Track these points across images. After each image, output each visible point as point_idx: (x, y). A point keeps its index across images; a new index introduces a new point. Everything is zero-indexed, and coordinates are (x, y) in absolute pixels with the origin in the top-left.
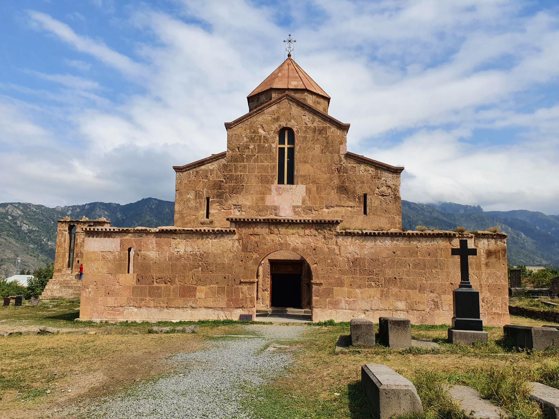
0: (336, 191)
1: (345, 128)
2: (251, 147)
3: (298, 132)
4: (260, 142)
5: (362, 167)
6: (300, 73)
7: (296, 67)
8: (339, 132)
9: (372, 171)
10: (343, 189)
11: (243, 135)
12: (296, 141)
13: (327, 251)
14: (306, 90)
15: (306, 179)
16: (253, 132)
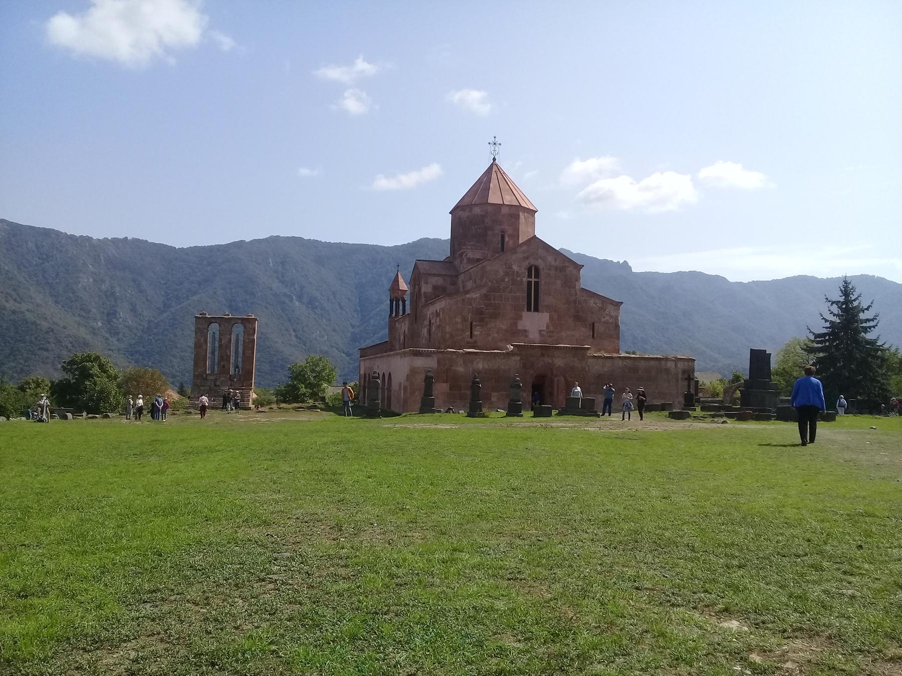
0: (572, 319)
1: (579, 267)
2: (507, 280)
3: (543, 269)
4: (514, 276)
5: (592, 301)
6: (509, 183)
7: (504, 176)
8: (575, 272)
9: (600, 304)
10: (578, 318)
11: (500, 270)
12: (542, 277)
13: (580, 368)
14: (519, 208)
15: (549, 308)
16: (509, 268)
